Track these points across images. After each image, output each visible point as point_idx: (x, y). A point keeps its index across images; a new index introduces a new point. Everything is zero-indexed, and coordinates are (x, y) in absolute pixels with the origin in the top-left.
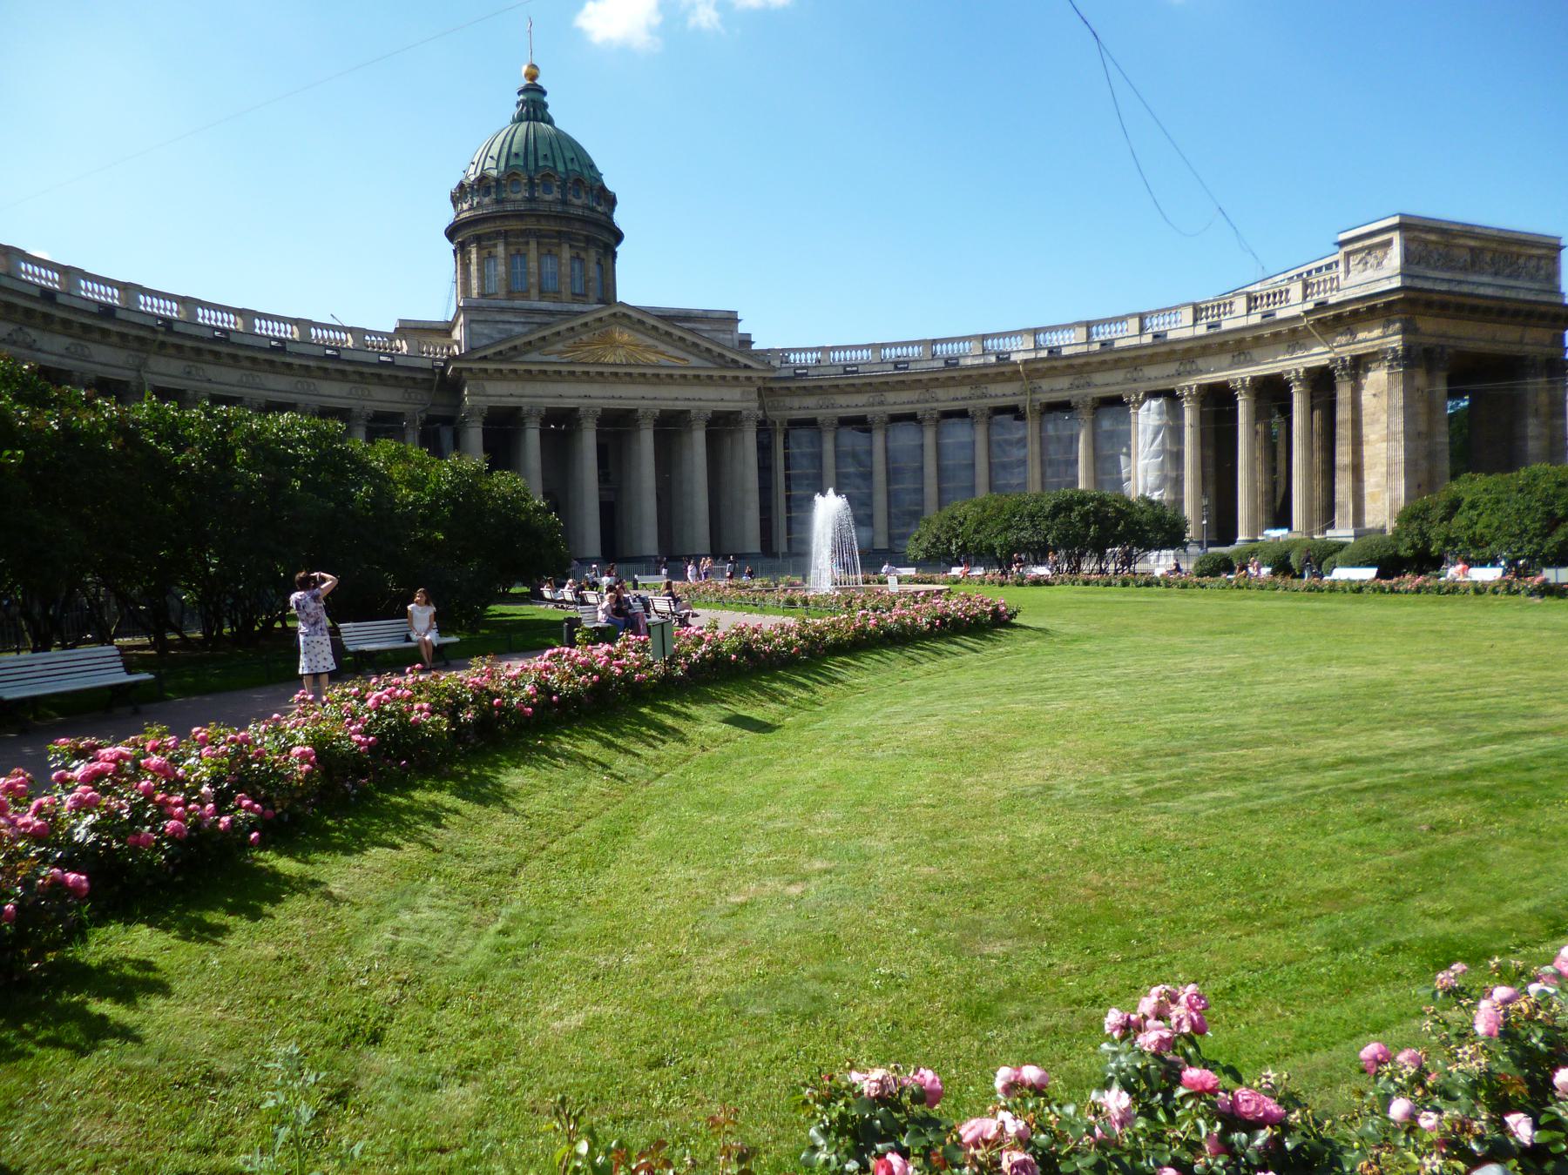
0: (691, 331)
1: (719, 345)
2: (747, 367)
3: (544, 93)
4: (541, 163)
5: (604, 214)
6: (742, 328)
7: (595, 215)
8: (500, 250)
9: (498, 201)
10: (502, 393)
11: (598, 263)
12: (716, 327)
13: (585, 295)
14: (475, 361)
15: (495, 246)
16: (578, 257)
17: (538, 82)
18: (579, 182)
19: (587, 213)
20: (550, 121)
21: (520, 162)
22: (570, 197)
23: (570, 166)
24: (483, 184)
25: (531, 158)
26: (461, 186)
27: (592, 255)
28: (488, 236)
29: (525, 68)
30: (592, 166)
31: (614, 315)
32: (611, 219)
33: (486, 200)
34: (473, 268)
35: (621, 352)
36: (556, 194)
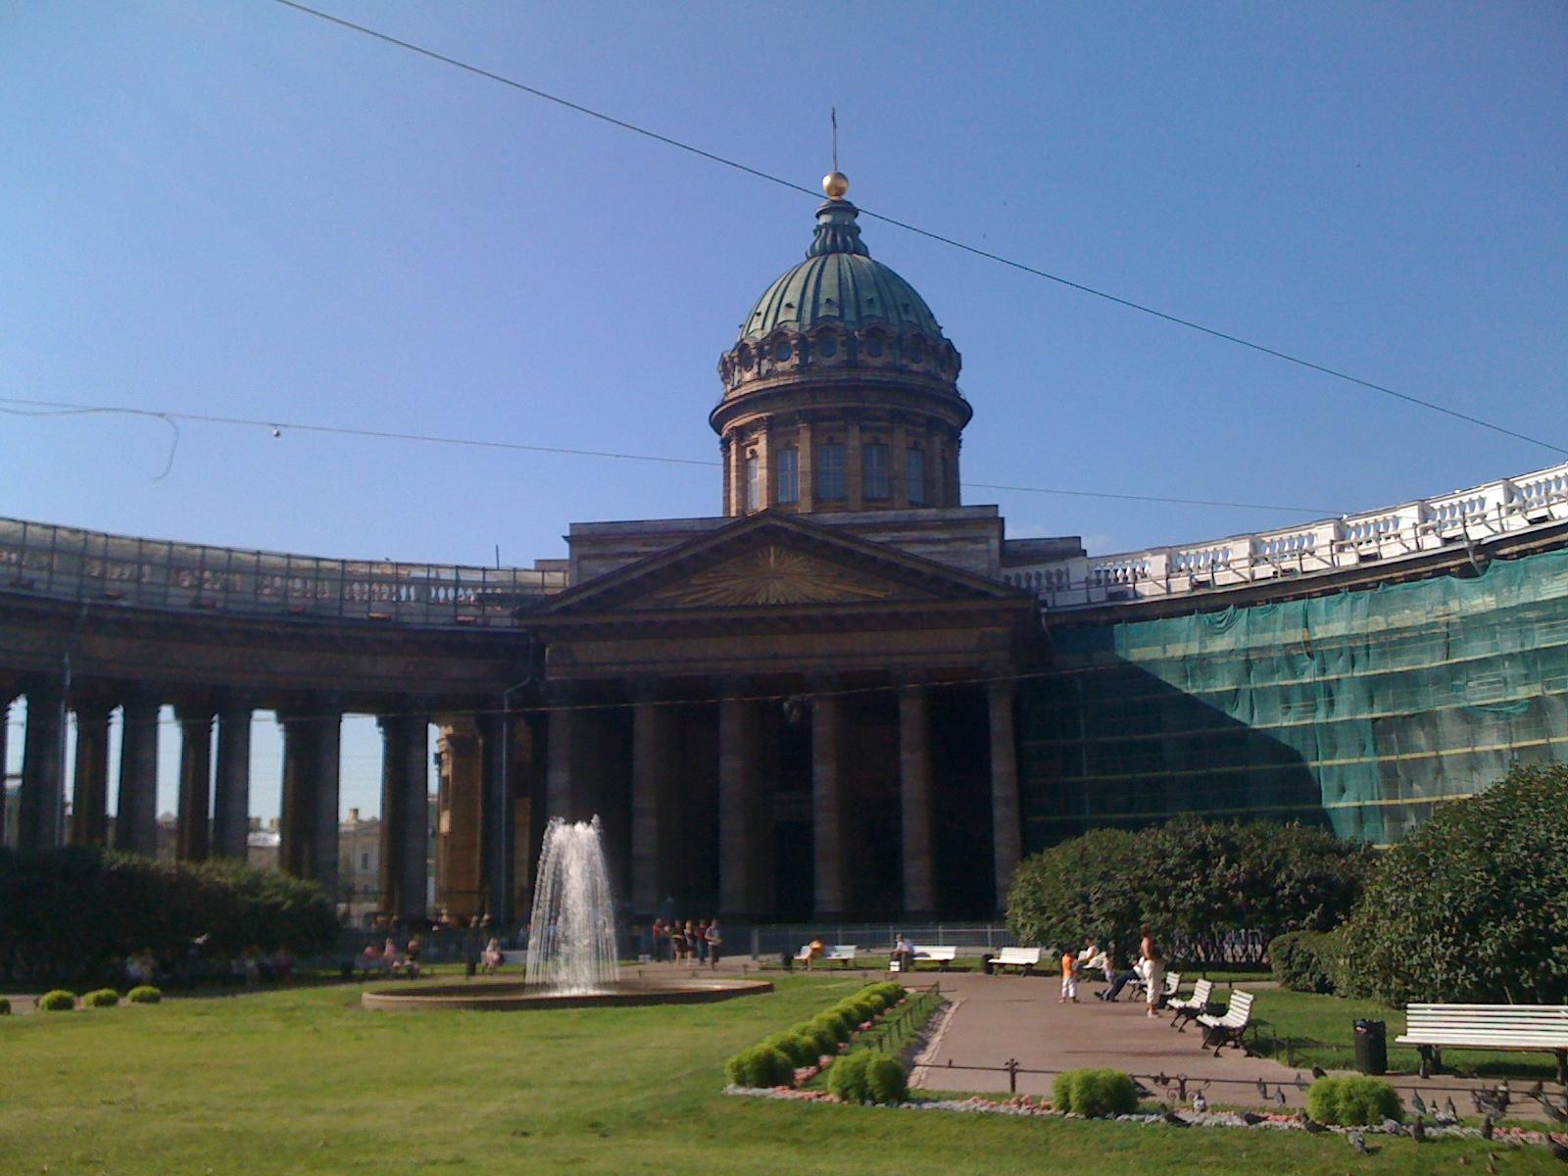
0: (877, 546)
1: (929, 563)
2: (983, 595)
3: (855, 212)
4: (821, 315)
5: (926, 374)
6: (1010, 534)
7: (902, 379)
8: (762, 448)
9: (759, 377)
10: (601, 656)
11: (915, 447)
12: (958, 533)
13: (889, 499)
14: (550, 615)
15: (756, 442)
16: (876, 441)
17: (845, 197)
18: (875, 334)
19: (890, 376)
20: (861, 249)
21: (792, 315)
22: (860, 357)
23: (865, 312)
24: (744, 355)
25: (808, 307)
26: (724, 363)
27: (900, 440)
28: (751, 428)
29: (827, 181)
30: (909, 301)
31: (762, 529)
32: (954, 385)
33: (748, 376)
34: (733, 475)
35: (779, 585)
36: (841, 355)
